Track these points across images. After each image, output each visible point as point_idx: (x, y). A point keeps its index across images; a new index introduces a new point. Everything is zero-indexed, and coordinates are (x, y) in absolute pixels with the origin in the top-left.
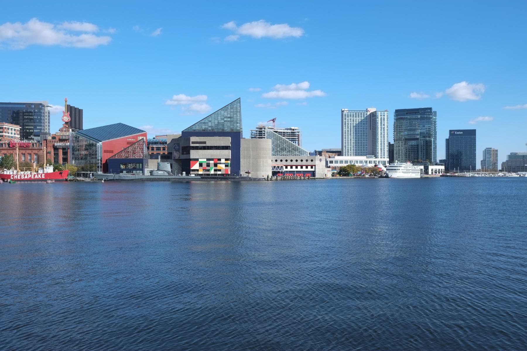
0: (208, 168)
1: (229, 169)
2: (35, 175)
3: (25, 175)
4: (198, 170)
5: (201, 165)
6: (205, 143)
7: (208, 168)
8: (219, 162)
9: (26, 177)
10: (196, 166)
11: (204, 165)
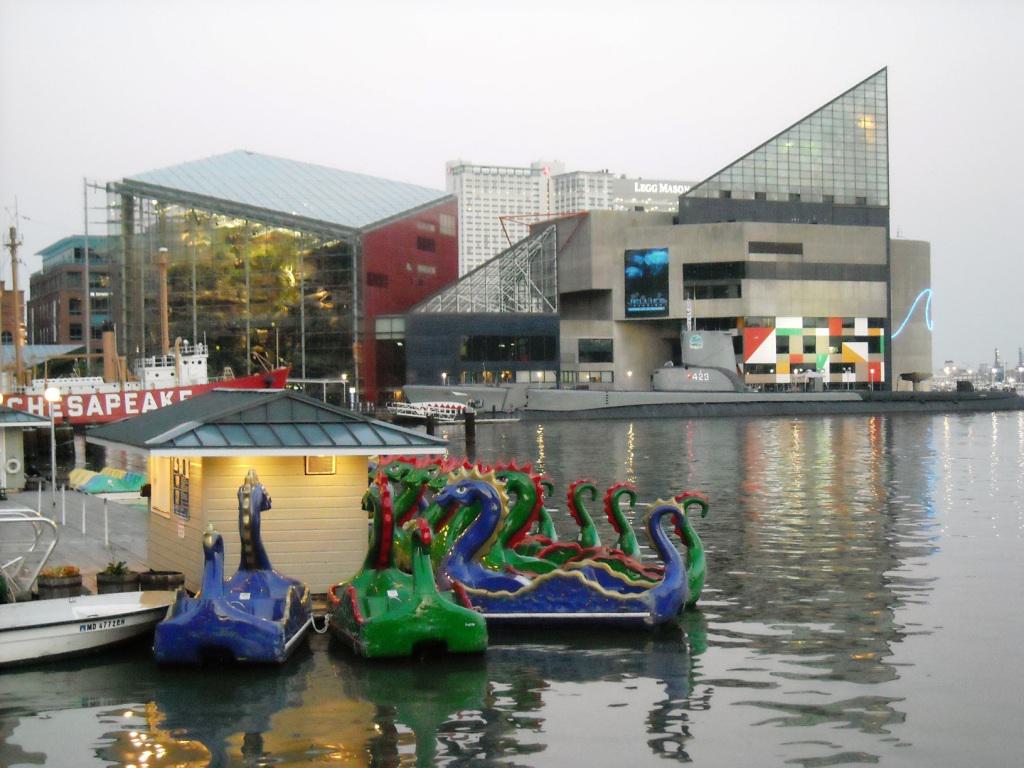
0: (808, 358)
1: (880, 358)
2: (141, 395)
3: (86, 399)
4: (766, 369)
5: (783, 347)
6: (796, 249)
7: (808, 358)
8: (846, 332)
9: (95, 408)
10: (765, 352)
11: (796, 347)
